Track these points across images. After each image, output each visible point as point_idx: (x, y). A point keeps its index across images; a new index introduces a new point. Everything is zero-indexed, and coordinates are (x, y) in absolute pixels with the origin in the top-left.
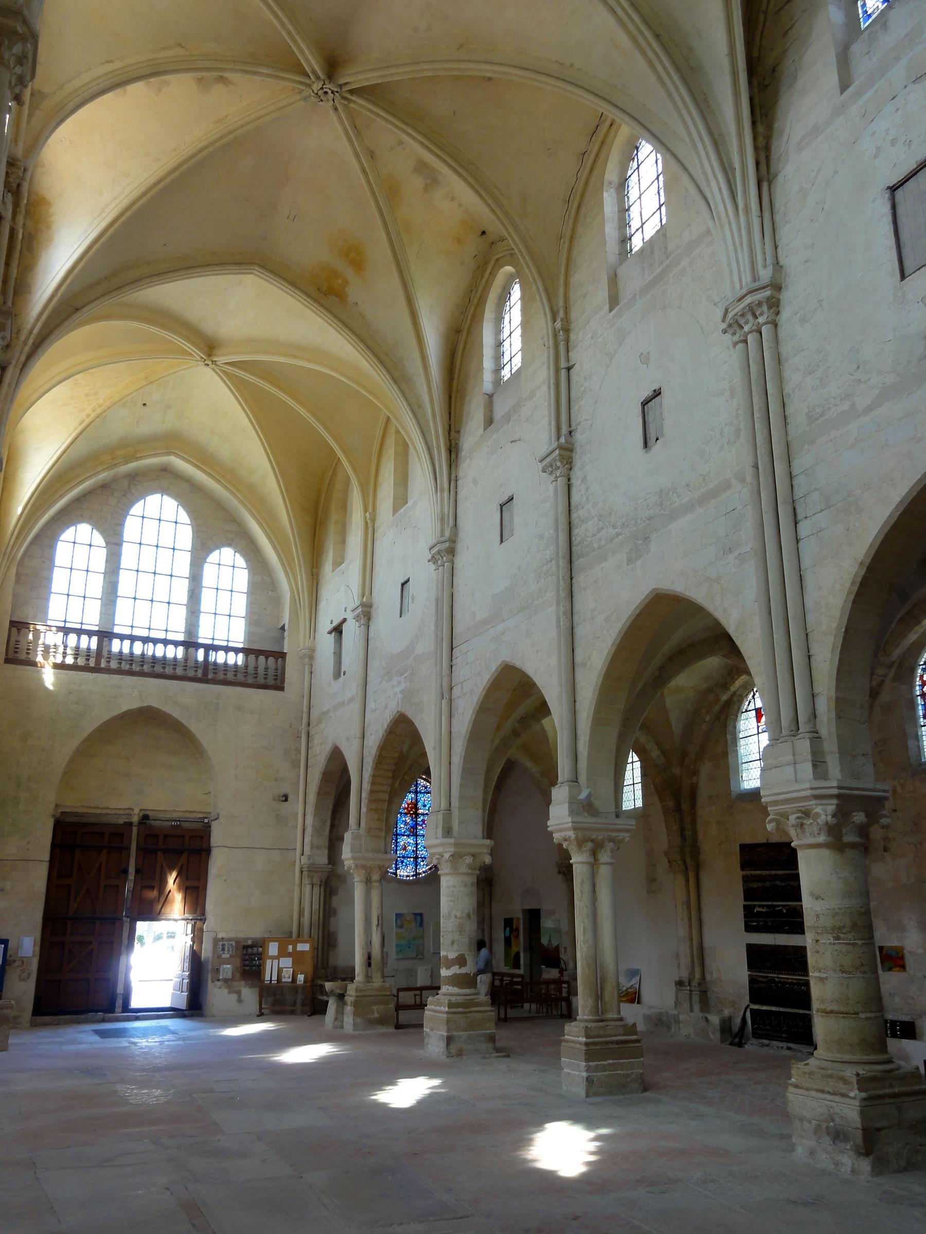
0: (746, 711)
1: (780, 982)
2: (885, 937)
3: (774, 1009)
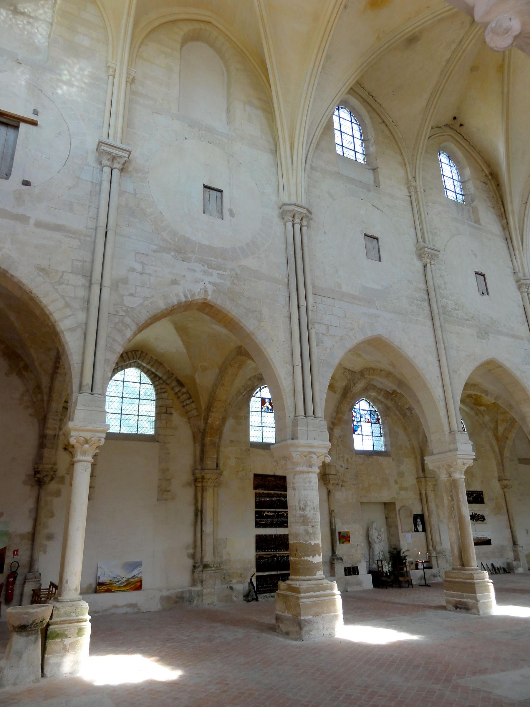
0: (254, 397)
1: (279, 556)
2: (340, 527)
3: (273, 573)
